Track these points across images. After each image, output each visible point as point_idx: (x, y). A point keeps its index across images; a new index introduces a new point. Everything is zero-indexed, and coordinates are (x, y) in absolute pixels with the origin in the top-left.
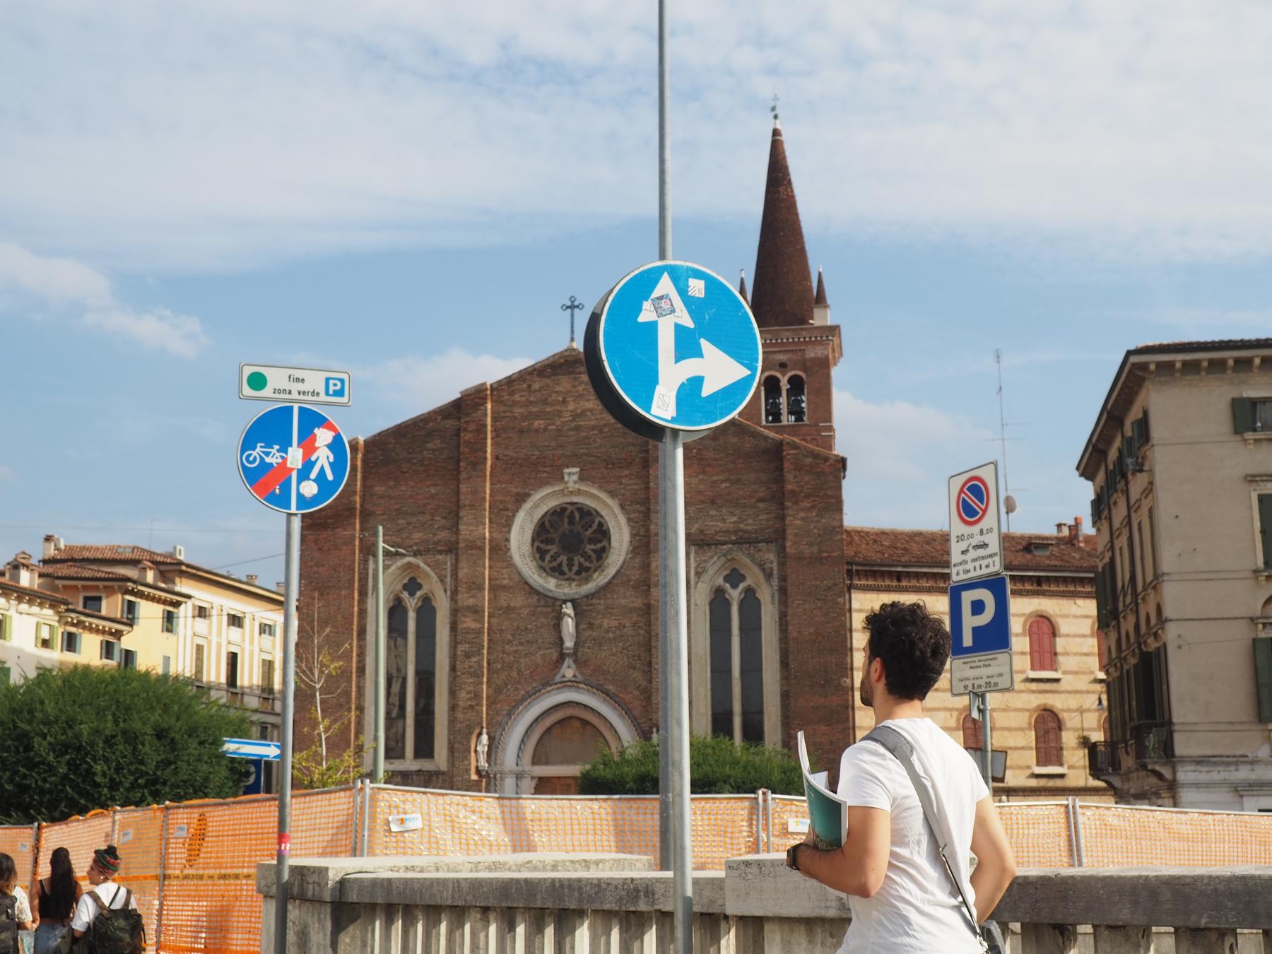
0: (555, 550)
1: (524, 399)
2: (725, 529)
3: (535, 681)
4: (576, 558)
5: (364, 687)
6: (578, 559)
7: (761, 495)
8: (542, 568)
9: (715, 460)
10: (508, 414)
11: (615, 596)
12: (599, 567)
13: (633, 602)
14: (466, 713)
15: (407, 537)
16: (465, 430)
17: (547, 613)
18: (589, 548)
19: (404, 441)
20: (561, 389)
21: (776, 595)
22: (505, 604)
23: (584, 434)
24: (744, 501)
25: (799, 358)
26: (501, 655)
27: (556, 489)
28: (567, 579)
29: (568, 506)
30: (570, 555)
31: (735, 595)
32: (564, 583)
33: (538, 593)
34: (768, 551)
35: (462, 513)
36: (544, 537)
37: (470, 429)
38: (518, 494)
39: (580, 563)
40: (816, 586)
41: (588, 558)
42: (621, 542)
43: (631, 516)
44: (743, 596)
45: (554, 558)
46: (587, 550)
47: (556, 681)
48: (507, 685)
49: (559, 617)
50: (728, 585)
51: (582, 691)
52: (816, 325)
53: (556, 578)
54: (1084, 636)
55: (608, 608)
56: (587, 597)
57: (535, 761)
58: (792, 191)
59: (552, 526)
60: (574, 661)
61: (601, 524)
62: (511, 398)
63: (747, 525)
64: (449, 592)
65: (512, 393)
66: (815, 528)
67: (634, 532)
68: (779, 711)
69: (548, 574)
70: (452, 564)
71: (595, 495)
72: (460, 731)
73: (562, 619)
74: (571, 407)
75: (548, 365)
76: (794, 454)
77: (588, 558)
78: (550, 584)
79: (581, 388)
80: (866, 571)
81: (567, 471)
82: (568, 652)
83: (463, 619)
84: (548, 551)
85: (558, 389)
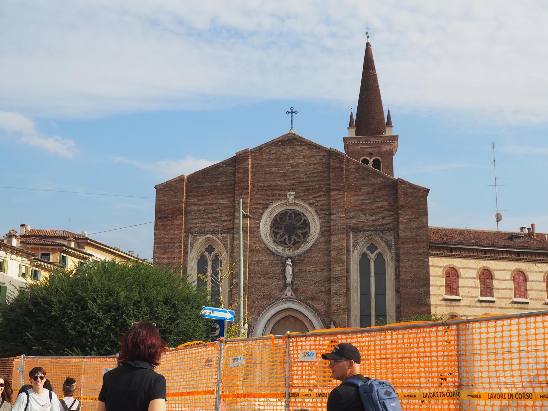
0: (283, 233)
1: (267, 157)
2: (368, 224)
3: (272, 297)
4: (292, 237)
7: (386, 207)
8: (275, 241)
9: (363, 189)
10: (259, 165)
11: (312, 256)
12: (304, 242)
16: (238, 172)
17: (278, 263)
18: (299, 232)
19: (207, 177)
21: (394, 257)
22: (257, 259)
23: (297, 175)
24: (377, 210)
25: (379, 150)
26: (255, 284)
29: (289, 211)
30: (290, 235)
31: (372, 257)
33: (274, 254)
37: (240, 171)
38: (264, 204)
39: (294, 239)
41: (299, 237)
42: (315, 229)
43: (321, 216)
44: (376, 257)
45: (281, 237)
46: (298, 233)
49: (284, 266)
50: (369, 252)
51: (295, 303)
52: (386, 135)
53: (282, 247)
54: (540, 282)
55: (308, 262)
56: (298, 256)
58: (375, 72)
59: (281, 220)
61: (305, 220)
62: (261, 157)
64: (229, 252)
65: (262, 154)
66: (414, 224)
68: (395, 315)
69: (279, 245)
70: (230, 238)
71: (303, 206)
73: (286, 267)
75: (280, 141)
76: (403, 187)
77: (299, 237)
78: (280, 249)
80: (435, 247)
81: (288, 193)
82: (289, 283)
84: (278, 233)
85: (284, 152)
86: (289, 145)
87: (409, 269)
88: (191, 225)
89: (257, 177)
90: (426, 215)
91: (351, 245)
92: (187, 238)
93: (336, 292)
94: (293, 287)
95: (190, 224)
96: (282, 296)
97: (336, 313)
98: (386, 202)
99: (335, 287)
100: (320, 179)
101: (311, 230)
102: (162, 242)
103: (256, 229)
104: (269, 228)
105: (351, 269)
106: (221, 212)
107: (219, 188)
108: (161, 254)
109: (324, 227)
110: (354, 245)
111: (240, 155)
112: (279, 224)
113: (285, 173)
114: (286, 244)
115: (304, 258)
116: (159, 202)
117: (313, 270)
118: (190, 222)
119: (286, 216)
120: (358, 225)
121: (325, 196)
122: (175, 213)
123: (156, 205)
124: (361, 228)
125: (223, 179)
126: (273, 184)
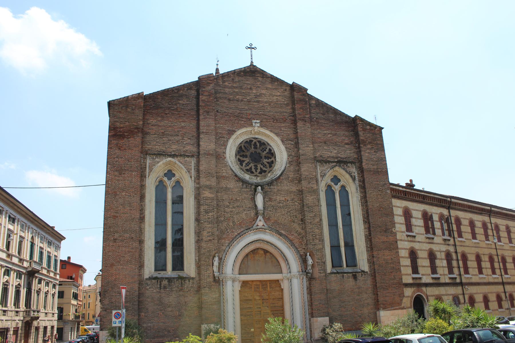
0: (248, 161)
3: (243, 227)
4: (258, 165)
5: (144, 229)
6: (259, 166)
7: (346, 141)
9: (325, 124)
10: (222, 91)
11: (282, 185)
12: (271, 171)
14: (207, 244)
15: (168, 147)
16: (202, 95)
18: (265, 161)
20: (249, 83)
22: (224, 186)
24: (339, 144)
26: (223, 213)
27: (249, 130)
28: (255, 176)
30: (256, 164)
31: (337, 188)
32: (253, 177)
35: (202, 136)
36: (242, 153)
41: (265, 166)
43: (287, 146)
46: (264, 162)
48: (227, 229)
50: (333, 184)
55: (278, 190)
61: (270, 150)
64: (193, 178)
65: (224, 82)
66: (374, 157)
68: (365, 244)
69: (245, 172)
71: (268, 135)
72: (204, 254)
75: (242, 71)
77: (265, 166)
78: (247, 177)
79: (259, 83)
81: (255, 121)
83: (203, 192)
84: (244, 161)
85: (247, 82)
86: (252, 76)
87: (375, 200)
88: (149, 147)
89: (221, 102)
90: (383, 150)
91: (319, 175)
92: (144, 160)
93: (310, 221)
96: (254, 226)
98: (346, 137)
99: (309, 216)
100: (284, 110)
101: (277, 159)
103: (222, 154)
104: (234, 155)
105: (321, 200)
106: (183, 135)
107: (180, 110)
109: (291, 157)
110: (321, 176)
111: (204, 78)
112: (244, 152)
113: (249, 101)
114: (252, 173)
115: (274, 187)
117: (284, 200)
118: (148, 143)
119: (251, 144)
120: (323, 157)
121: (290, 127)
122: (132, 131)
123: (110, 121)
126: (237, 111)
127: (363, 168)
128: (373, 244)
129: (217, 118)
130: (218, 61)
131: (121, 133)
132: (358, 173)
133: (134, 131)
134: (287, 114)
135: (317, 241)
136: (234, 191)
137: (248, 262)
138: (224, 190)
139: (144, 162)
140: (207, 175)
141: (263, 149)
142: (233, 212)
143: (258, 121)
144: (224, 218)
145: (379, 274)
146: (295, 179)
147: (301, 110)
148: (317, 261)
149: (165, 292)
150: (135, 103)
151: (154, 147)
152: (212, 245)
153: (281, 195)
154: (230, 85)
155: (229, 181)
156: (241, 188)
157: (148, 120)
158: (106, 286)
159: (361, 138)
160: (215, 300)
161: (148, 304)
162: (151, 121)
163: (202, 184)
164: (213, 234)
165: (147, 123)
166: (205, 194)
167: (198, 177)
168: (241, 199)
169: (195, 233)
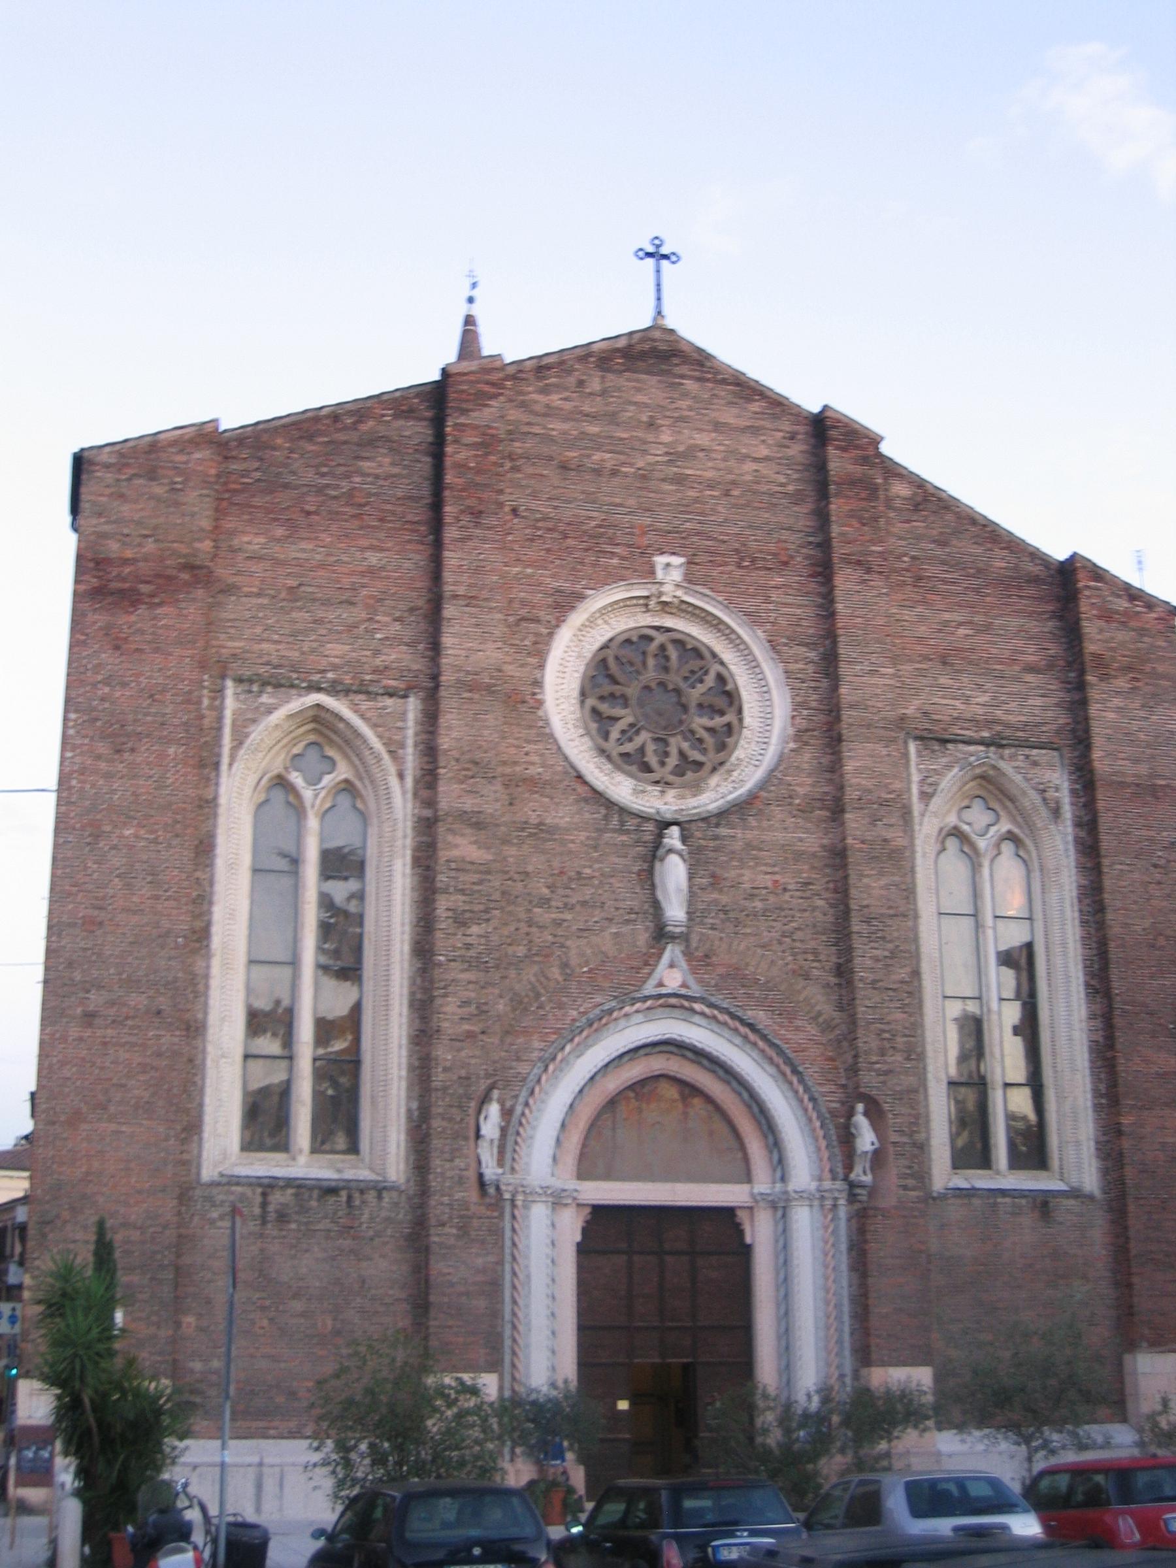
0: (630, 719)
2: (968, 716)
3: (601, 989)
5: (207, 976)
6: (676, 743)
7: (1032, 658)
8: (602, 752)
9: (945, 581)
10: (536, 430)
12: (721, 764)
13: (801, 840)
14: (459, 1050)
16: (456, 441)
18: (700, 722)
20: (645, 399)
22: (534, 819)
23: (692, 493)
26: (524, 928)
28: (657, 782)
32: (650, 788)
34: (1051, 766)
35: (449, 611)
36: (608, 688)
40: (1151, 840)
45: (628, 734)
46: (694, 726)
47: (646, 993)
48: (538, 995)
55: (749, 846)
57: (584, 1173)
60: (684, 953)
61: (721, 679)
63: (1007, 712)
64: (409, 781)
67: (799, 699)
69: (618, 768)
72: (445, 1089)
73: (662, 860)
74: (666, 437)
75: (618, 350)
79: (684, 404)
82: (678, 930)
83: (450, 838)
85: (639, 398)
87: (1135, 902)
88: (236, 644)
92: (214, 699)
94: (687, 947)
95: (231, 639)
97: (878, 1066)
98: (1030, 638)
101: (748, 720)
102: (103, 699)
103: (530, 689)
104: (576, 693)
106: (372, 602)
108: (99, 757)
109: (805, 712)
113: (644, 477)
114: (647, 768)
116: (94, 521)
117: (769, 884)
122: (170, 578)
124: (945, 730)
125: (380, 463)
127: (1091, 771)
128: (1120, 1081)
129: (510, 538)
130: (474, 285)
131: (127, 585)
132: (1073, 792)
133: (176, 578)
134: (794, 537)
135: (899, 1057)
136: (573, 842)
137: (614, 1129)
138: (531, 835)
139: (211, 707)
140: (468, 769)
141: (693, 672)
142: (565, 924)
143: (677, 560)
144: (529, 950)
145: (1142, 1202)
146: (818, 804)
147: (854, 522)
148: (894, 1138)
149: (284, 1237)
150: (184, 463)
151: (256, 647)
152: (477, 1053)
153: (757, 864)
154: (568, 406)
155: (552, 798)
156: (598, 830)
157: (233, 533)
158: (48, 1202)
159: (1090, 647)
160: (480, 1278)
161: (209, 1282)
162: (246, 539)
163: (444, 804)
164: (482, 1011)
165: (230, 546)
166: (456, 846)
167: (428, 779)
168: (597, 874)
169: (412, 1004)
